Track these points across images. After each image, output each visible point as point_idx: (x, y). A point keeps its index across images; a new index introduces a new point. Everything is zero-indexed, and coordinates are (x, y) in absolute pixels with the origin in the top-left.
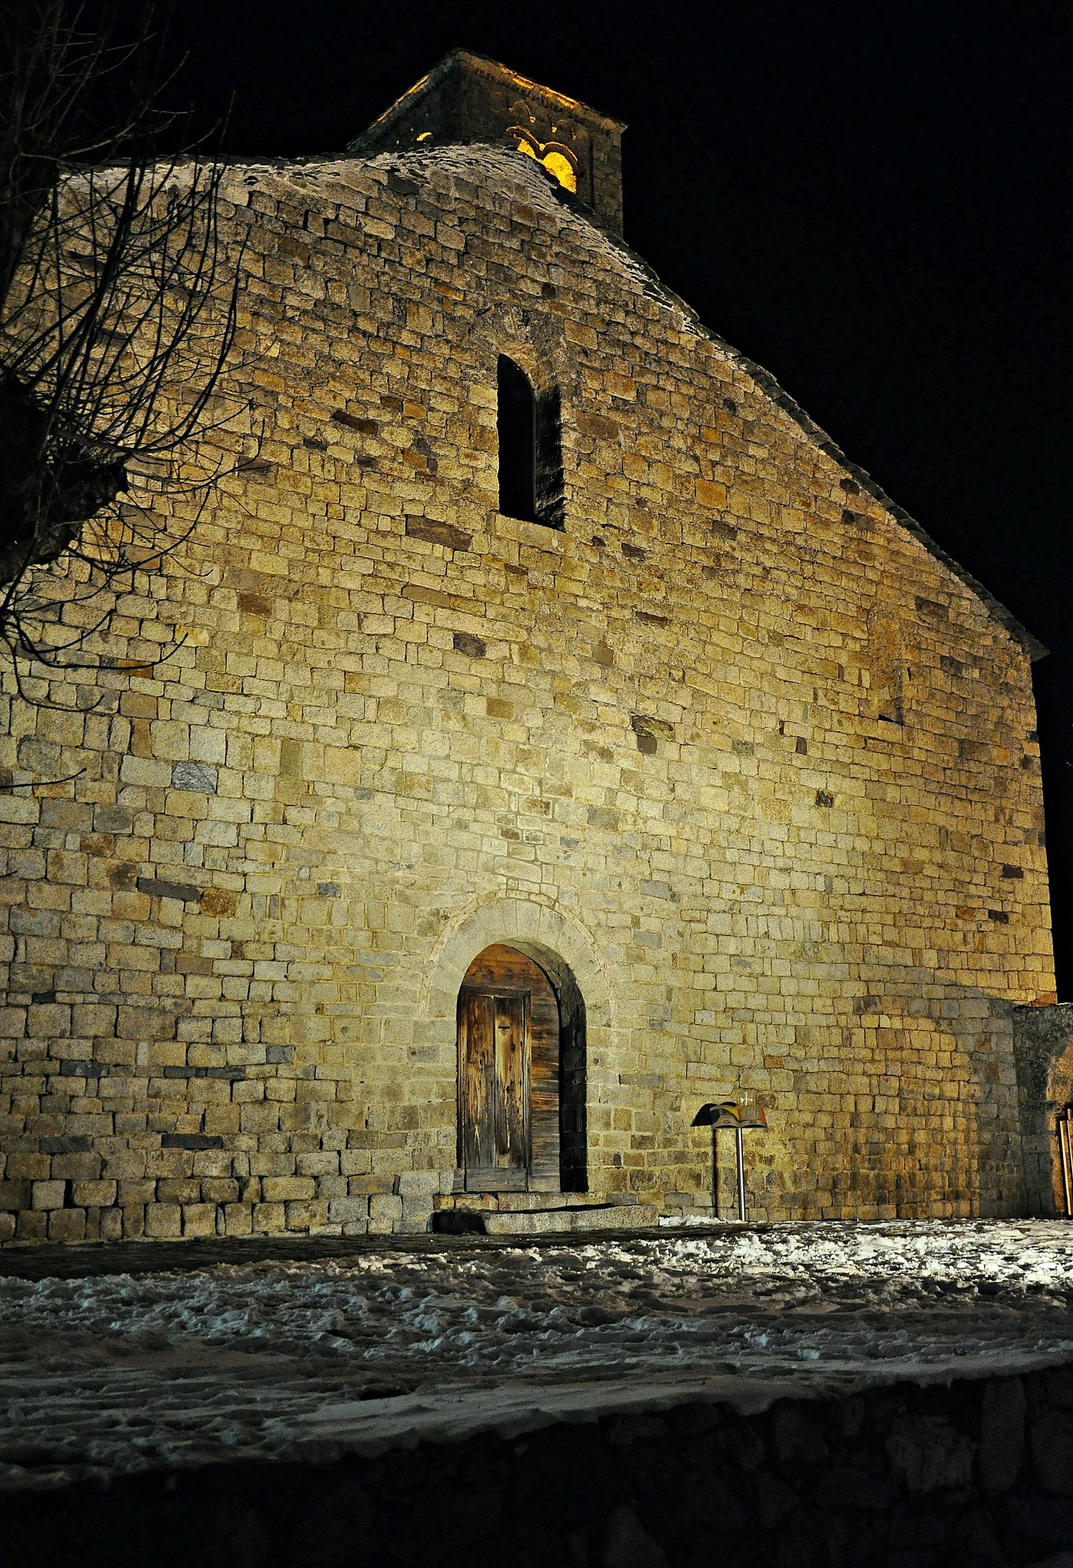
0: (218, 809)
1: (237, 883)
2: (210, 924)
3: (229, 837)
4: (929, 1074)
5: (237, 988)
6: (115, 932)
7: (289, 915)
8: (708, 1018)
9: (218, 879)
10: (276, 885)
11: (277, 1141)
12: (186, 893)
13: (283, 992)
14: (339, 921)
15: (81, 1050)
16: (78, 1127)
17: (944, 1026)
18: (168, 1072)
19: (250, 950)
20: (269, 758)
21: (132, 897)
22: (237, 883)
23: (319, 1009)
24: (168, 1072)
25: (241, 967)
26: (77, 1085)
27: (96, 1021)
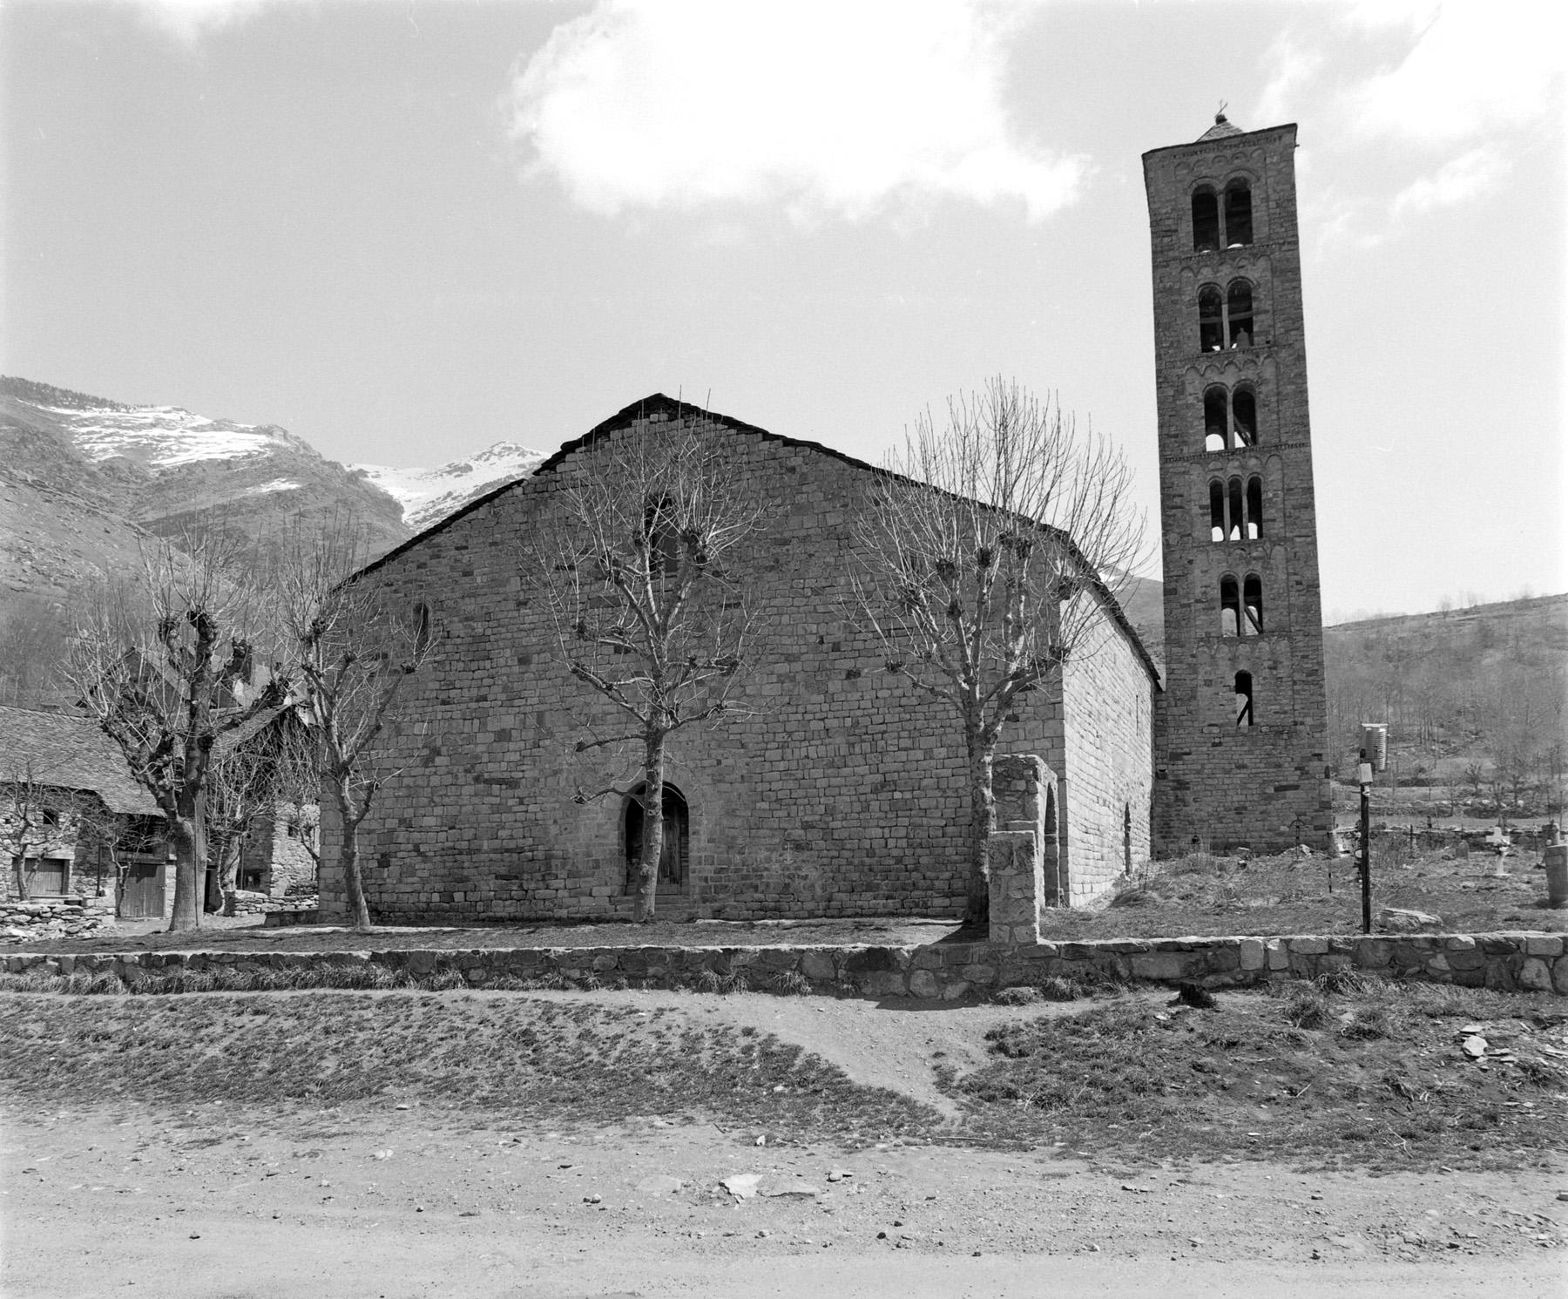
0: (512, 746)
1: (521, 775)
2: (510, 792)
3: (515, 757)
4: (933, 822)
5: (520, 816)
6: (476, 800)
7: (541, 785)
8: (765, 805)
9: (513, 774)
10: (536, 773)
11: (538, 876)
12: (500, 782)
13: (539, 816)
14: (563, 784)
15: (464, 845)
16: (466, 873)
17: (950, 793)
18: (495, 851)
19: (525, 802)
20: (532, 720)
21: (481, 786)
22: (521, 775)
23: (555, 822)
24: (495, 851)
25: (523, 808)
26: (464, 857)
27: (469, 834)
